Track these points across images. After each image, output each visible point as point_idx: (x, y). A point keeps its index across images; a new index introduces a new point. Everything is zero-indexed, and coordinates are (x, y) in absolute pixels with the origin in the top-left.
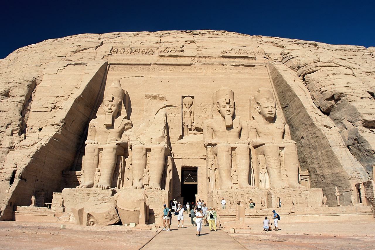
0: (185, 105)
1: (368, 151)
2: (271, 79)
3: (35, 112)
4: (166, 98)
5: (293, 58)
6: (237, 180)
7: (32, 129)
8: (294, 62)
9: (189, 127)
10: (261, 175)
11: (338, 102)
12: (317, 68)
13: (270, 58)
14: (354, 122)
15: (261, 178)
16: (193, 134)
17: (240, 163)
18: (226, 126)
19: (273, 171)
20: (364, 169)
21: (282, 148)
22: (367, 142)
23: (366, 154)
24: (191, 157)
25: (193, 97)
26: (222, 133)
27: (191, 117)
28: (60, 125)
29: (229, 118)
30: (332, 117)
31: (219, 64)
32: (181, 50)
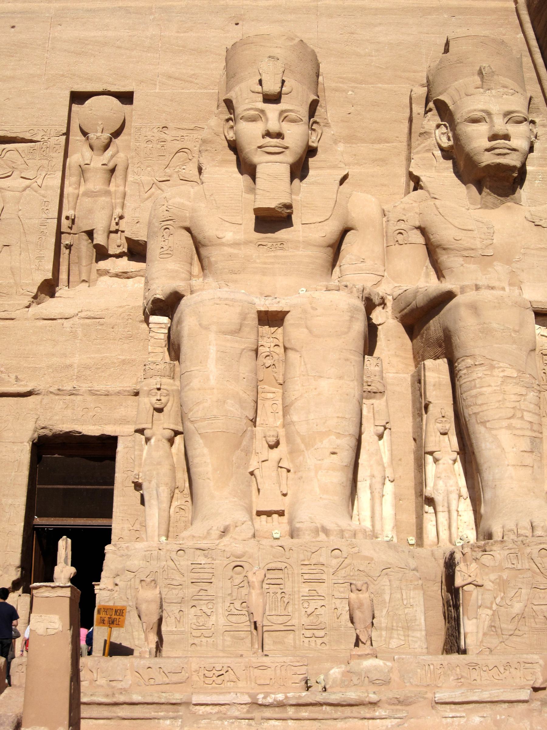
0: (85, 134)
6: (285, 495)
9: (100, 239)
10: (430, 467)
15: (429, 491)
16: (117, 275)
18: (257, 211)
19: (495, 437)
24: (84, 387)
25: (126, 98)
26: (235, 251)
27: (108, 193)
29: (273, 171)
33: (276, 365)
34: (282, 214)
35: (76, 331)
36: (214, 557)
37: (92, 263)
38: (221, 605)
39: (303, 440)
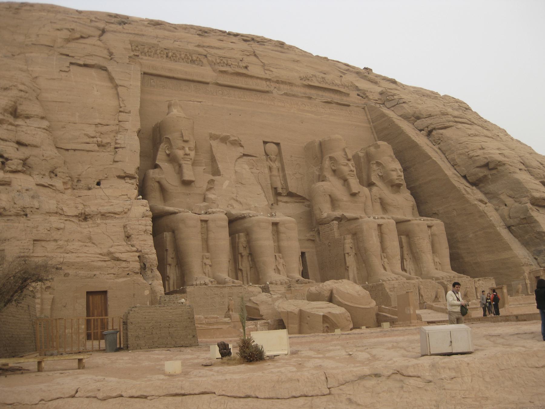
1: (539, 233)
2: (373, 129)
3: (67, 150)
5: (404, 103)
7: (79, 181)
8: (408, 109)
11: (494, 172)
12: (451, 124)
13: (367, 97)
14: (517, 198)
20: (530, 255)
21: (429, 227)
22: (538, 222)
23: (535, 237)
25: (278, 144)
28: (135, 178)
30: (483, 189)
31: (305, 97)
32: (244, 65)
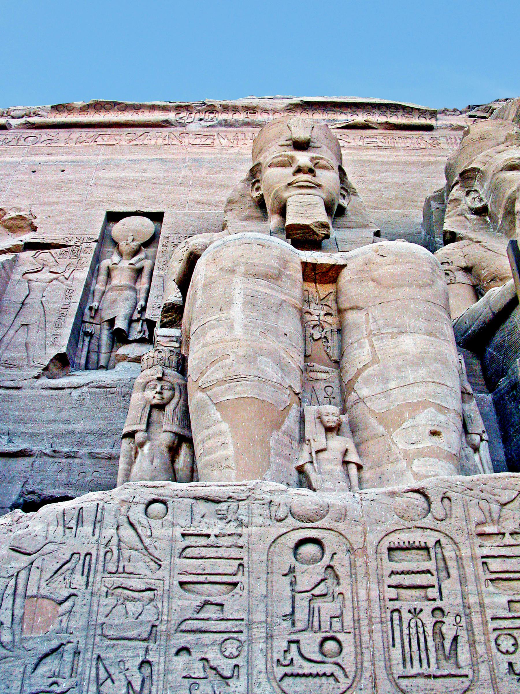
4: (33, 220)
17: (375, 361)
24: (84, 451)
25: (157, 217)
33: (329, 338)
34: (318, 235)
35: (84, 399)
36: (245, 520)
37: (111, 352)
38: (262, 645)
39: (381, 419)
